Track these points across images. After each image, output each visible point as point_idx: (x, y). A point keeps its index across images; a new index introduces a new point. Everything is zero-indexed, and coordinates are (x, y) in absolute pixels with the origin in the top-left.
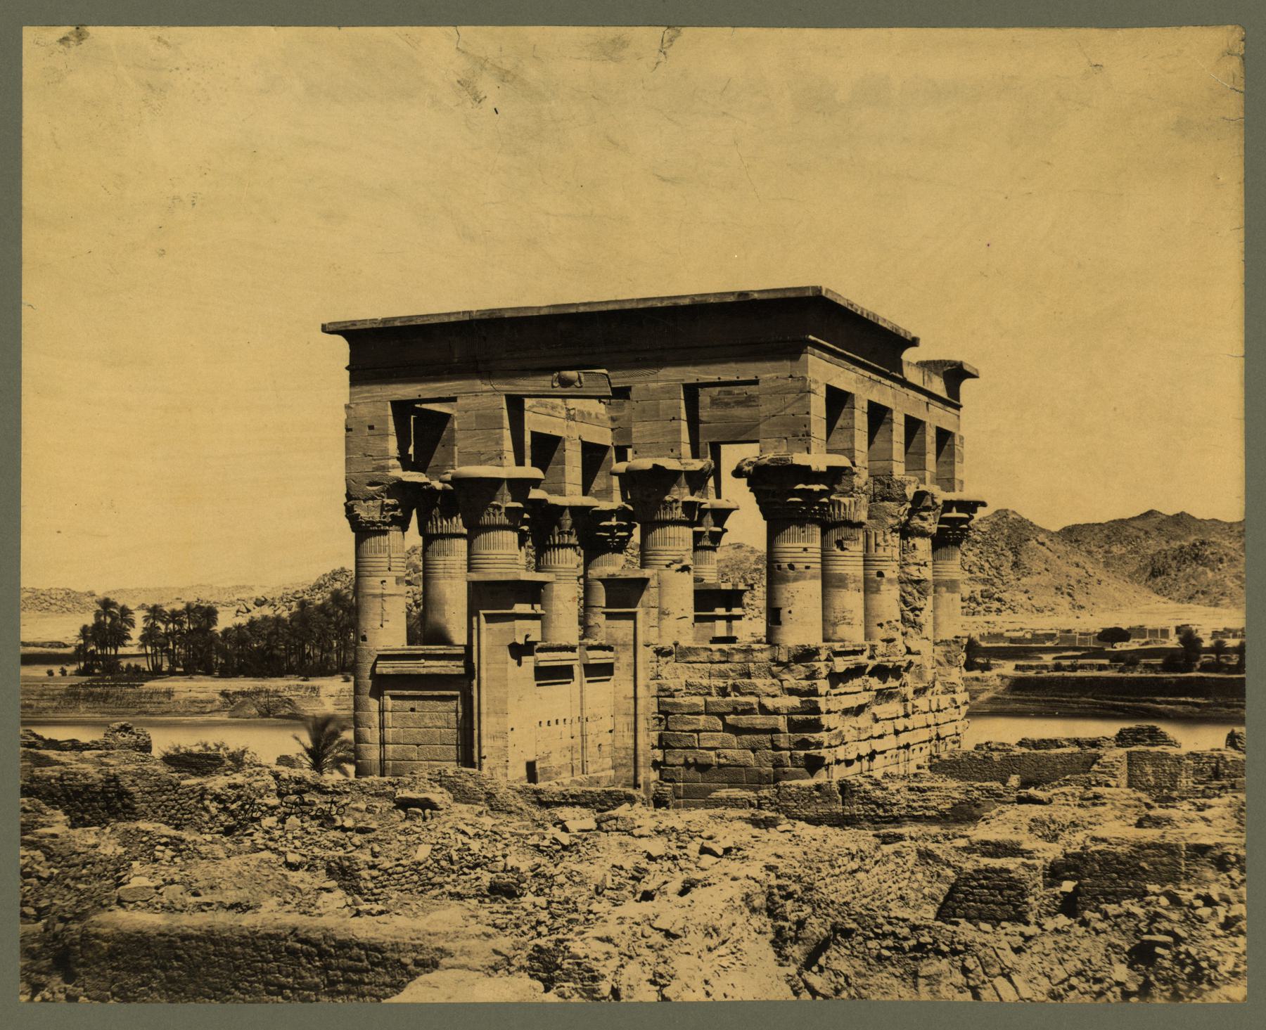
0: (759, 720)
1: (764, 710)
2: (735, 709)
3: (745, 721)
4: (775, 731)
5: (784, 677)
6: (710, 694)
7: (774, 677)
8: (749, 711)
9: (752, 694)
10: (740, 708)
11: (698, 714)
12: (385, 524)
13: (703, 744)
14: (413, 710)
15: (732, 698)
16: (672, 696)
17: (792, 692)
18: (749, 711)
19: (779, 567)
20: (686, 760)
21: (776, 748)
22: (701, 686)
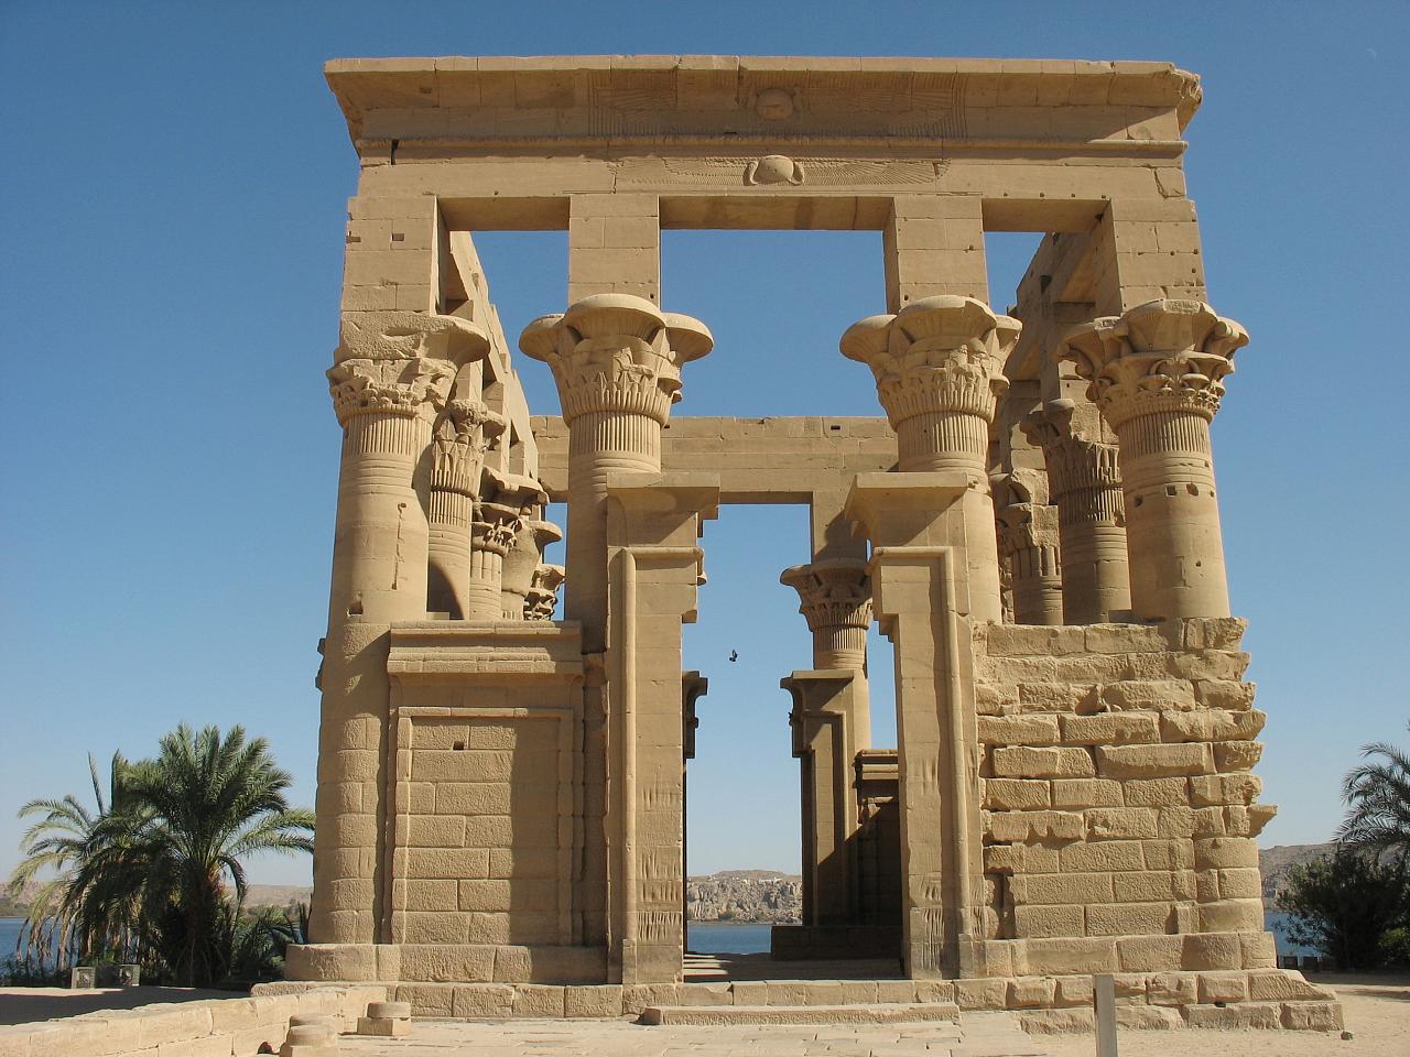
0: (1166, 753)
1: (1169, 732)
3: (1135, 753)
4: (1197, 771)
6: (1067, 708)
9: (1146, 705)
11: (1049, 744)
14: (459, 747)
15: (1110, 714)
16: (1001, 714)
17: (1218, 701)
19: (1172, 491)
21: (1195, 800)
22: (1053, 696)
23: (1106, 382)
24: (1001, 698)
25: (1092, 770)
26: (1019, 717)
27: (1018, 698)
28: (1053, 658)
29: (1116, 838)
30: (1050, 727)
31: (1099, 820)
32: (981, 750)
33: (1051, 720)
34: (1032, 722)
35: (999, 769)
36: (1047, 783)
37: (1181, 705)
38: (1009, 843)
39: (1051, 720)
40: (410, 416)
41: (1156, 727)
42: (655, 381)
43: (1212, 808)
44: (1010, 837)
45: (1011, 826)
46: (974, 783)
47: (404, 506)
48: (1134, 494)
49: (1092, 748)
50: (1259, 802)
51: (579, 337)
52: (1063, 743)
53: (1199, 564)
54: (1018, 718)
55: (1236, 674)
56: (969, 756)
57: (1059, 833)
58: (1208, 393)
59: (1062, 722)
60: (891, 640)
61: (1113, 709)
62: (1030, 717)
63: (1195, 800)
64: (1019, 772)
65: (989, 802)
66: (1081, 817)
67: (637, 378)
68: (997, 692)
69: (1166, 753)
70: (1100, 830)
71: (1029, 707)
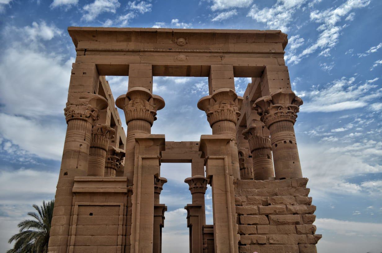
0: (290, 218)
2: (275, 211)
3: (281, 218)
4: (297, 223)
5: (298, 195)
6: (260, 204)
7: (291, 195)
8: (281, 213)
9: (282, 203)
10: (277, 211)
12: (86, 117)
13: (259, 231)
16: (242, 205)
18: (281, 213)
20: (252, 241)
21: (298, 232)
23: (266, 114)
24: (241, 200)
25: (268, 222)
26: (247, 206)
27: (246, 200)
28: (255, 189)
29: (276, 244)
30: (255, 209)
31: (270, 238)
32: (236, 215)
33: (255, 207)
34: (250, 208)
35: (242, 222)
36: (255, 226)
37: (292, 203)
38: (245, 245)
39: (255, 207)
40: (86, 121)
41: (285, 210)
42: (149, 112)
43: (303, 235)
44: (246, 243)
45: (247, 240)
46: (234, 226)
47: (81, 145)
48: (275, 144)
49: (267, 216)
50: (317, 233)
51: (130, 99)
52: (260, 214)
53: (294, 163)
54: (245, 207)
55: (306, 194)
56: (233, 217)
57: (260, 242)
58: (294, 116)
59: (259, 208)
60: (211, 186)
61: (273, 204)
62: (250, 206)
63: (298, 232)
64: (248, 223)
65: (239, 232)
66: (265, 237)
67: (144, 111)
68: (240, 199)
69: (290, 218)
70: (271, 241)
71: (248, 203)
